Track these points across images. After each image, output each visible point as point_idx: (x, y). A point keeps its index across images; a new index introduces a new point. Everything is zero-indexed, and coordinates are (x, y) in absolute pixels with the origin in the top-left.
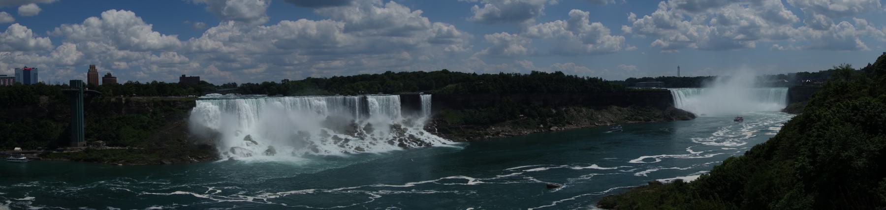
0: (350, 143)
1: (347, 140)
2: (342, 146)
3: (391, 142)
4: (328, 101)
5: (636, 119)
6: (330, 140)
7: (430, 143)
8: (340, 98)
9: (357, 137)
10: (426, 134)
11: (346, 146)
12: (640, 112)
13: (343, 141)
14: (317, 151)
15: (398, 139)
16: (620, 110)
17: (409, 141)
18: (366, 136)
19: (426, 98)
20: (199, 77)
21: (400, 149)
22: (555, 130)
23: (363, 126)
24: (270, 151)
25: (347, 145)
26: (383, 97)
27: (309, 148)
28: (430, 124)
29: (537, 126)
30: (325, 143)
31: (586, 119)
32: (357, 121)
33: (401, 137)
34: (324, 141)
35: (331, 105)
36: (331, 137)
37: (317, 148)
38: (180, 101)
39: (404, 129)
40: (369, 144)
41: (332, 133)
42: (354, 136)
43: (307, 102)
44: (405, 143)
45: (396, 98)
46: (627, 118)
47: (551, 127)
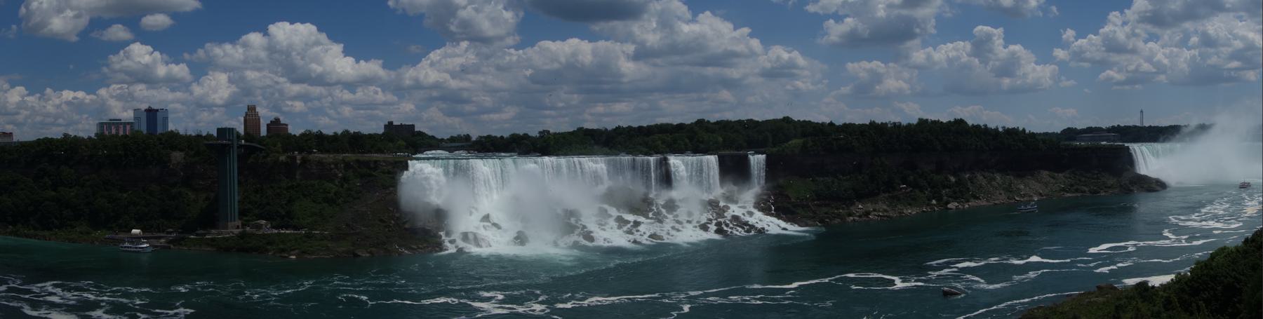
0: (642, 228)
1: (637, 224)
2: (630, 232)
3: (704, 227)
4: (608, 164)
5: (1077, 191)
6: (612, 223)
7: (763, 229)
8: (626, 159)
9: (651, 218)
10: (758, 214)
11: (636, 233)
12: (1083, 179)
13: (632, 224)
14: (591, 239)
15: (714, 222)
16: (1053, 178)
17: (731, 226)
18: (667, 218)
19: (757, 160)
20: (413, 126)
21: (717, 237)
22: (954, 207)
23: (661, 202)
24: (520, 239)
25: (638, 231)
26: (692, 159)
27: (579, 235)
28: (764, 199)
29: (927, 202)
30: (603, 227)
31: (1002, 192)
32: (651, 196)
33: (719, 220)
34: (602, 225)
35: (616, 170)
36: (614, 218)
37: (592, 234)
38: (384, 161)
39: (724, 206)
40: (670, 229)
41: (614, 212)
42: (647, 217)
43: (578, 166)
44: (725, 228)
45: (712, 160)
46: (1063, 190)
47: (948, 203)
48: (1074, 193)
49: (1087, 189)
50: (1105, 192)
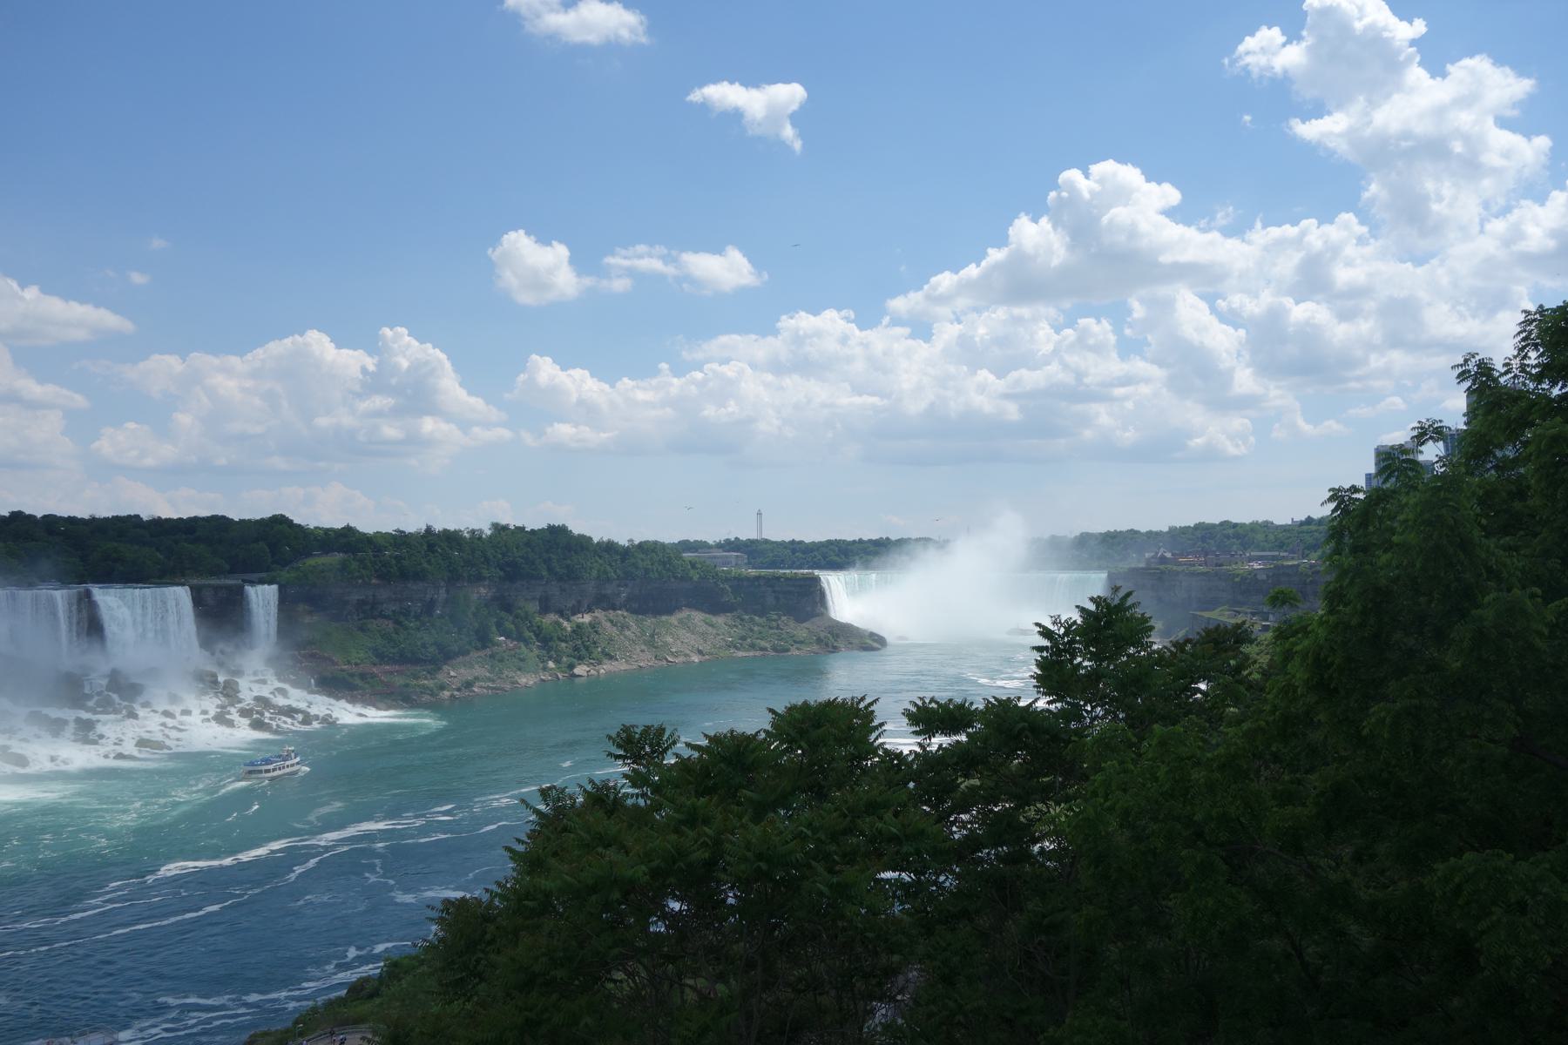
5: (753, 646)
12: (756, 628)
16: (712, 626)
22: (585, 674)
29: (541, 665)
31: (643, 647)
47: (571, 667)
48: (748, 650)
49: (768, 645)
50: (798, 649)
